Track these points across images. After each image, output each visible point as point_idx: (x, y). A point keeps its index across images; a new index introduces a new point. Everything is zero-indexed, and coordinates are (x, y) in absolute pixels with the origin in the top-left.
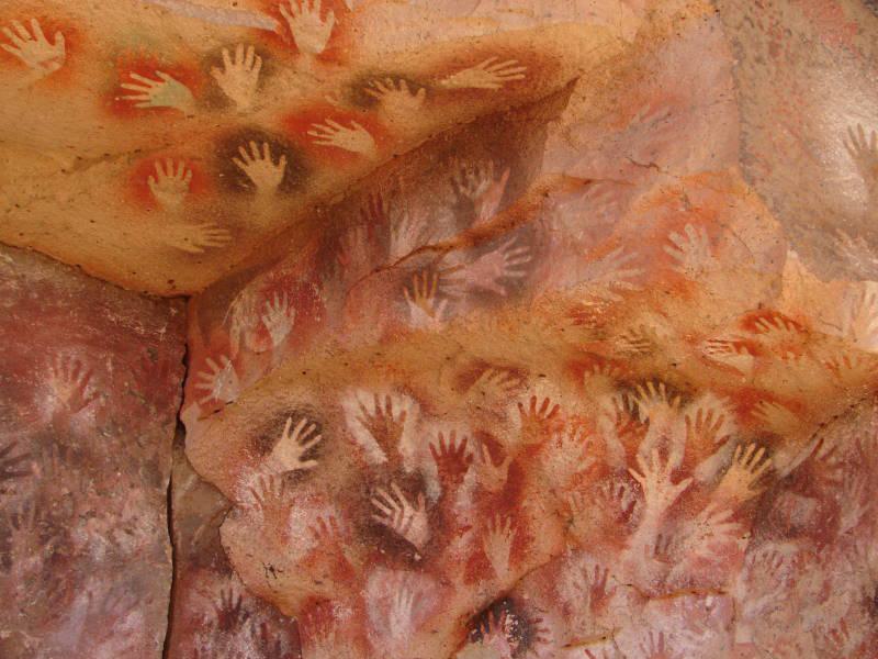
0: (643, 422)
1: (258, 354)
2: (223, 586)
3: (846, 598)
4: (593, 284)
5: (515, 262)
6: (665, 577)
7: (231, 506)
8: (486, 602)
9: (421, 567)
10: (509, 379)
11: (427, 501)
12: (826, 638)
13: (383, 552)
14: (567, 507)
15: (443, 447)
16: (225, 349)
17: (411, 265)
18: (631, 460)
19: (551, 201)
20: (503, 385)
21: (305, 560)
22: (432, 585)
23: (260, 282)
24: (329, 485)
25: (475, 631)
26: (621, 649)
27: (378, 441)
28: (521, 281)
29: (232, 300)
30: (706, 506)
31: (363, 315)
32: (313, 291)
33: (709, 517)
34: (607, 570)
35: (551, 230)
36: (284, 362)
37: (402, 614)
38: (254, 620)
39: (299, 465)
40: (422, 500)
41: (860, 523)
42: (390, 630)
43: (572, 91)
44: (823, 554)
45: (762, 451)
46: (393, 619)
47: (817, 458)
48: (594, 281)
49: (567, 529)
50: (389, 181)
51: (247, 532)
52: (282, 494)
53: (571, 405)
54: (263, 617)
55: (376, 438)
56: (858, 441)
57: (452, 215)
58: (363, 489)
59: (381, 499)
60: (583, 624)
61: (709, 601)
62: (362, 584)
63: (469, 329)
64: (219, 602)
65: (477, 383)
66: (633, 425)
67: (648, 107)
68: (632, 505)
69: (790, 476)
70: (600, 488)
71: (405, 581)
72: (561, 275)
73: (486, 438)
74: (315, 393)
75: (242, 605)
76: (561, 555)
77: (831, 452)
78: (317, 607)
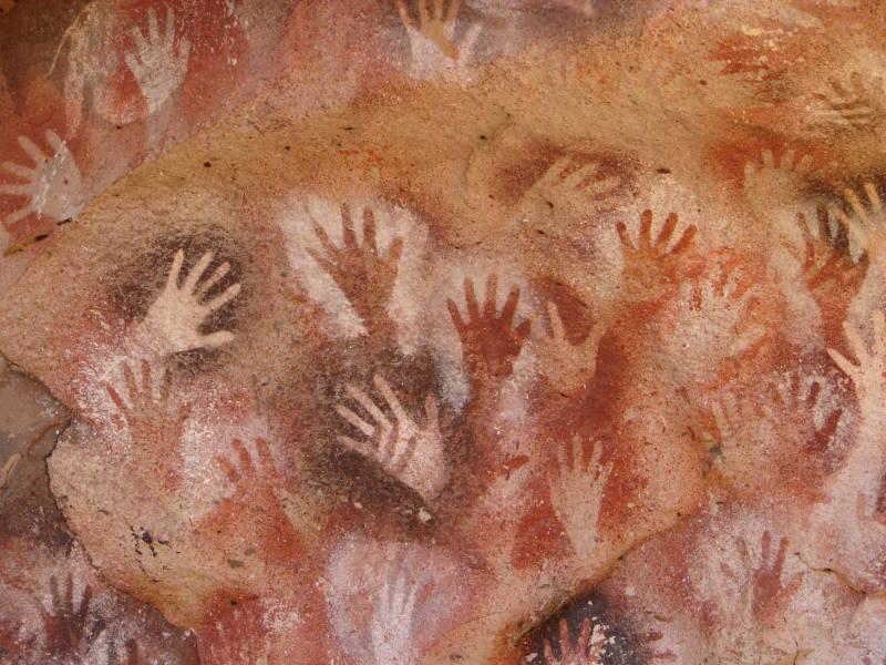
0: (855, 260)
2: (55, 570)
7: (69, 419)
8: (554, 601)
9: (430, 535)
10: (600, 177)
11: (443, 409)
13: (358, 505)
14: (707, 418)
15: (472, 306)
16: (56, 119)
18: (833, 332)
20: (588, 189)
21: (210, 521)
22: (451, 568)
24: (255, 379)
25: (534, 655)
27: (349, 296)
29: (67, 24)
34: (784, 542)
36: (169, 143)
37: (395, 622)
38: (115, 633)
39: (198, 342)
40: (432, 405)
46: (377, 634)
51: (101, 468)
52: (165, 396)
53: (718, 227)
54: (131, 627)
55: (344, 288)
58: (320, 386)
59: (353, 406)
62: (319, 566)
63: (525, 81)
64: (48, 601)
65: (539, 184)
66: (836, 264)
68: (833, 418)
70: (771, 385)
73: (555, 290)
74: (227, 204)
75: (92, 605)
76: (697, 512)
78: (233, 605)
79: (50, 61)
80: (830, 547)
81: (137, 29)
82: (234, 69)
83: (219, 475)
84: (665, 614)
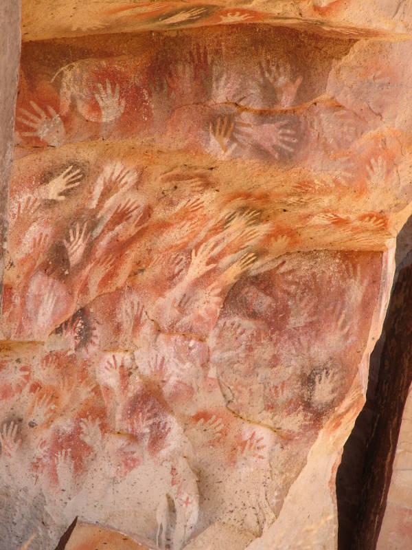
1: (87, 121)
3: (290, 370)
4: (329, 174)
5: (286, 139)
6: (177, 322)
9: (64, 279)
10: (199, 186)
12: (270, 390)
13: (50, 263)
17: (218, 109)
18: (197, 247)
19: (316, 109)
23: (95, 64)
26: (137, 361)
28: (290, 156)
29: (62, 66)
30: (212, 283)
31: (179, 131)
32: (142, 94)
33: (211, 290)
34: (143, 306)
35: (312, 126)
41: (306, 326)
42: (37, 319)
43: (352, 46)
44: (274, 336)
45: (255, 258)
46: (41, 312)
47: (278, 272)
48: (330, 172)
49: (135, 274)
50: (213, 42)
52: (36, 210)
56: (314, 275)
57: (259, 91)
60: (126, 340)
61: (192, 343)
67: (379, 73)
69: (256, 277)
71: (52, 286)
72: (314, 161)
77: (290, 272)
79: (52, 78)
80: (158, 313)
81: (100, 85)
82: (146, 122)
83: (31, 244)
84: (101, 323)
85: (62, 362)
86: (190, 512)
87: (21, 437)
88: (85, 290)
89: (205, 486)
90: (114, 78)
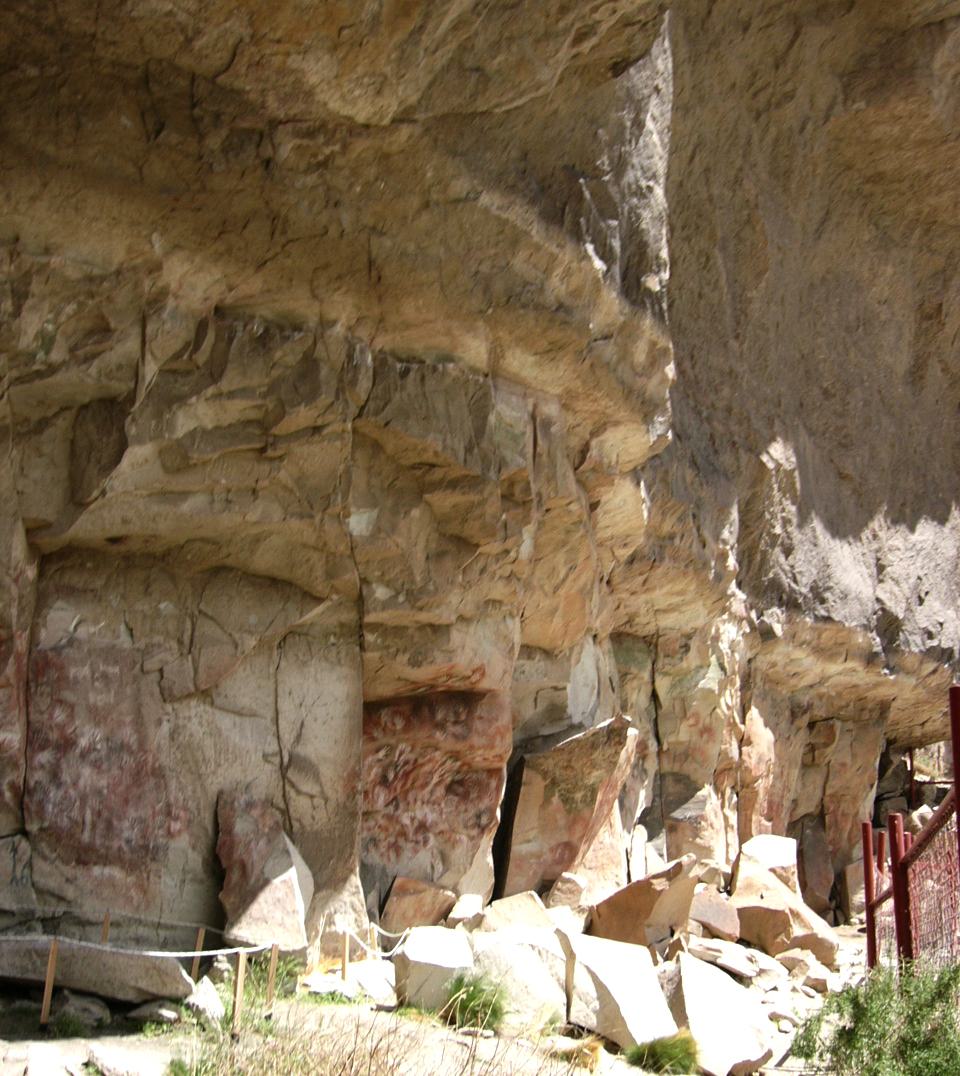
85: (390, 818)
86: (439, 867)
87: (376, 845)
88: (395, 790)
89: (444, 858)
90: (401, 714)
